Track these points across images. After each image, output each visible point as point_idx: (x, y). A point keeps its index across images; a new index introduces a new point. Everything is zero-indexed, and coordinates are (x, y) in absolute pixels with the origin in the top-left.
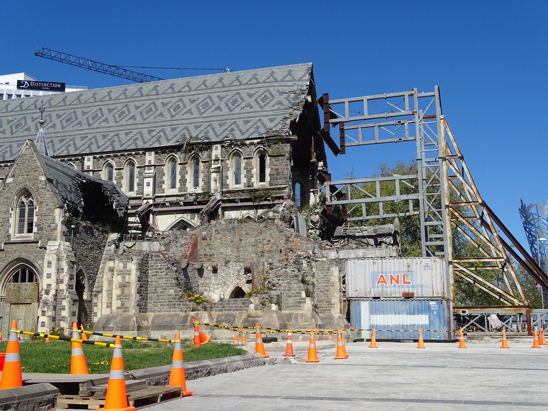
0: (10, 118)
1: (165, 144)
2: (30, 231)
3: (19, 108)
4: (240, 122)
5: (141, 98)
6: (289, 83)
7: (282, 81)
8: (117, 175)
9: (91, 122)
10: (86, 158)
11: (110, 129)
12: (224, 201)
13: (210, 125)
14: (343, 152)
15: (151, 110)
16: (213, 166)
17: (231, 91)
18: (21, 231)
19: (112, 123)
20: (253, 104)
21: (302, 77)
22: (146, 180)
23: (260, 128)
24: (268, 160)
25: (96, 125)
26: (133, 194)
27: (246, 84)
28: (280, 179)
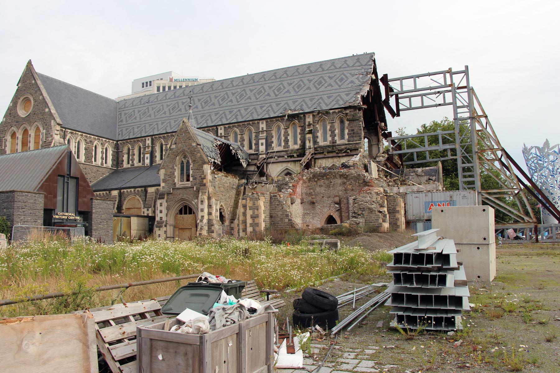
0: (168, 104)
2: (188, 180)
3: (173, 96)
4: (325, 97)
5: (254, 84)
6: (358, 68)
7: (353, 66)
8: (241, 138)
9: (221, 103)
10: (219, 128)
11: (234, 107)
13: (304, 101)
14: (398, 115)
15: (261, 92)
16: (307, 130)
17: (317, 75)
20: (333, 84)
21: (367, 63)
22: (260, 141)
23: (339, 101)
24: (347, 123)
25: (224, 104)
26: (252, 152)
27: (328, 70)
28: (355, 137)
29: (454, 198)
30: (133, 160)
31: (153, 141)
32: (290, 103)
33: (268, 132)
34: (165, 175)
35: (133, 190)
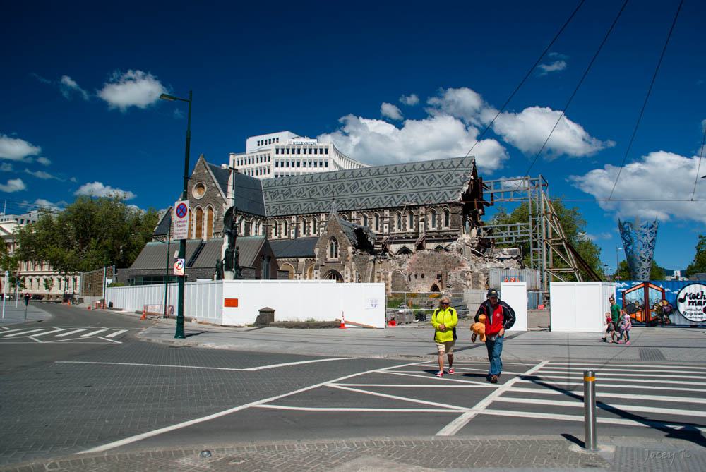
1: (394, 205)
2: (336, 256)
6: (462, 169)
12: (426, 237)
14: (493, 204)
18: (332, 256)
19: (364, 191)
20: (441, 182)
22: (385, 225)
24: (450, 215)
26: (378, 232)
29: (522, 274)
30: (280, 233)
31: (297, 218)
32: (408, 195)
33: (391, 218)
34: (319, 252)
35: (286, 259)
